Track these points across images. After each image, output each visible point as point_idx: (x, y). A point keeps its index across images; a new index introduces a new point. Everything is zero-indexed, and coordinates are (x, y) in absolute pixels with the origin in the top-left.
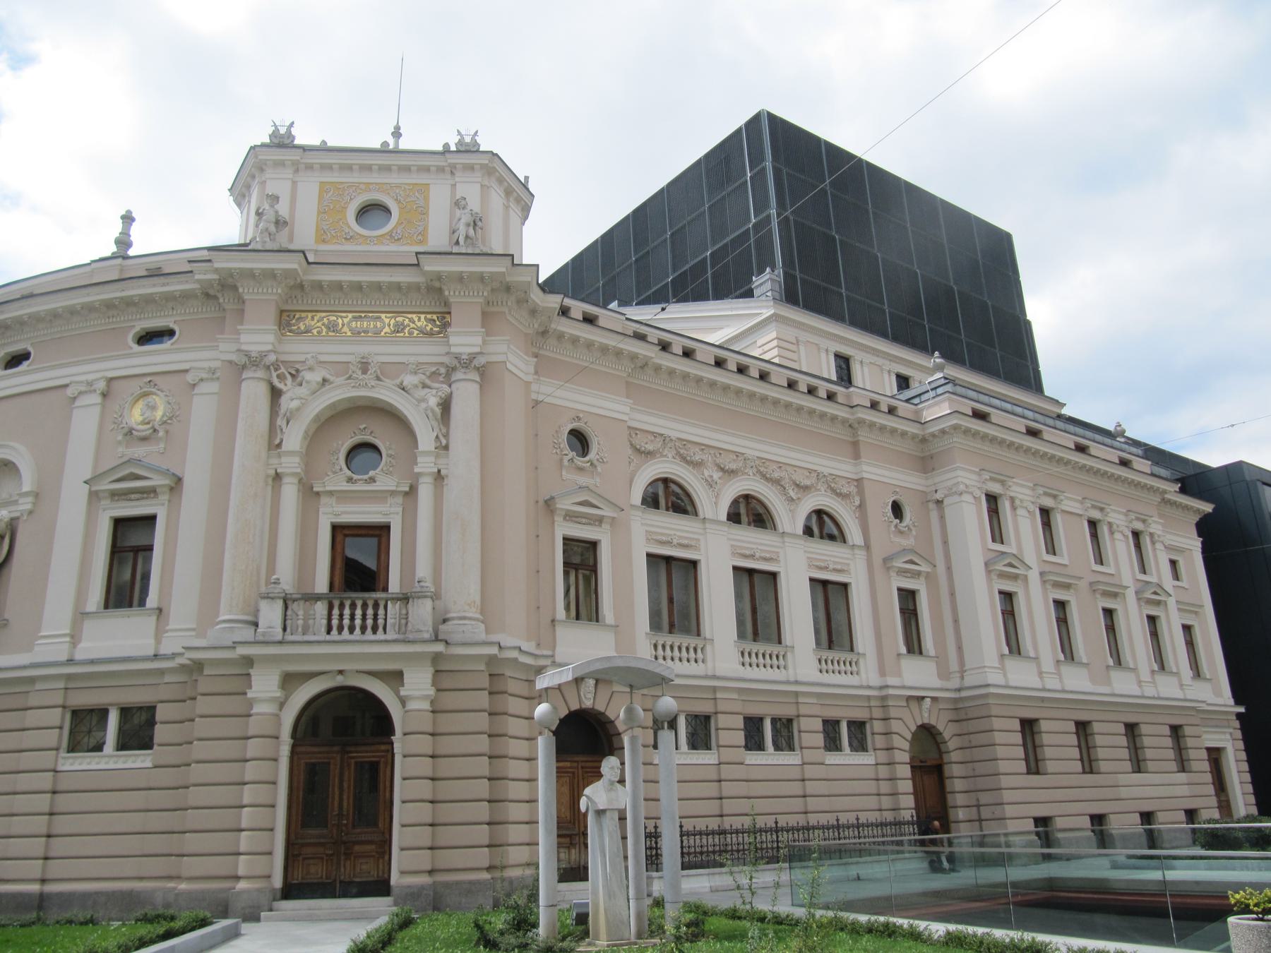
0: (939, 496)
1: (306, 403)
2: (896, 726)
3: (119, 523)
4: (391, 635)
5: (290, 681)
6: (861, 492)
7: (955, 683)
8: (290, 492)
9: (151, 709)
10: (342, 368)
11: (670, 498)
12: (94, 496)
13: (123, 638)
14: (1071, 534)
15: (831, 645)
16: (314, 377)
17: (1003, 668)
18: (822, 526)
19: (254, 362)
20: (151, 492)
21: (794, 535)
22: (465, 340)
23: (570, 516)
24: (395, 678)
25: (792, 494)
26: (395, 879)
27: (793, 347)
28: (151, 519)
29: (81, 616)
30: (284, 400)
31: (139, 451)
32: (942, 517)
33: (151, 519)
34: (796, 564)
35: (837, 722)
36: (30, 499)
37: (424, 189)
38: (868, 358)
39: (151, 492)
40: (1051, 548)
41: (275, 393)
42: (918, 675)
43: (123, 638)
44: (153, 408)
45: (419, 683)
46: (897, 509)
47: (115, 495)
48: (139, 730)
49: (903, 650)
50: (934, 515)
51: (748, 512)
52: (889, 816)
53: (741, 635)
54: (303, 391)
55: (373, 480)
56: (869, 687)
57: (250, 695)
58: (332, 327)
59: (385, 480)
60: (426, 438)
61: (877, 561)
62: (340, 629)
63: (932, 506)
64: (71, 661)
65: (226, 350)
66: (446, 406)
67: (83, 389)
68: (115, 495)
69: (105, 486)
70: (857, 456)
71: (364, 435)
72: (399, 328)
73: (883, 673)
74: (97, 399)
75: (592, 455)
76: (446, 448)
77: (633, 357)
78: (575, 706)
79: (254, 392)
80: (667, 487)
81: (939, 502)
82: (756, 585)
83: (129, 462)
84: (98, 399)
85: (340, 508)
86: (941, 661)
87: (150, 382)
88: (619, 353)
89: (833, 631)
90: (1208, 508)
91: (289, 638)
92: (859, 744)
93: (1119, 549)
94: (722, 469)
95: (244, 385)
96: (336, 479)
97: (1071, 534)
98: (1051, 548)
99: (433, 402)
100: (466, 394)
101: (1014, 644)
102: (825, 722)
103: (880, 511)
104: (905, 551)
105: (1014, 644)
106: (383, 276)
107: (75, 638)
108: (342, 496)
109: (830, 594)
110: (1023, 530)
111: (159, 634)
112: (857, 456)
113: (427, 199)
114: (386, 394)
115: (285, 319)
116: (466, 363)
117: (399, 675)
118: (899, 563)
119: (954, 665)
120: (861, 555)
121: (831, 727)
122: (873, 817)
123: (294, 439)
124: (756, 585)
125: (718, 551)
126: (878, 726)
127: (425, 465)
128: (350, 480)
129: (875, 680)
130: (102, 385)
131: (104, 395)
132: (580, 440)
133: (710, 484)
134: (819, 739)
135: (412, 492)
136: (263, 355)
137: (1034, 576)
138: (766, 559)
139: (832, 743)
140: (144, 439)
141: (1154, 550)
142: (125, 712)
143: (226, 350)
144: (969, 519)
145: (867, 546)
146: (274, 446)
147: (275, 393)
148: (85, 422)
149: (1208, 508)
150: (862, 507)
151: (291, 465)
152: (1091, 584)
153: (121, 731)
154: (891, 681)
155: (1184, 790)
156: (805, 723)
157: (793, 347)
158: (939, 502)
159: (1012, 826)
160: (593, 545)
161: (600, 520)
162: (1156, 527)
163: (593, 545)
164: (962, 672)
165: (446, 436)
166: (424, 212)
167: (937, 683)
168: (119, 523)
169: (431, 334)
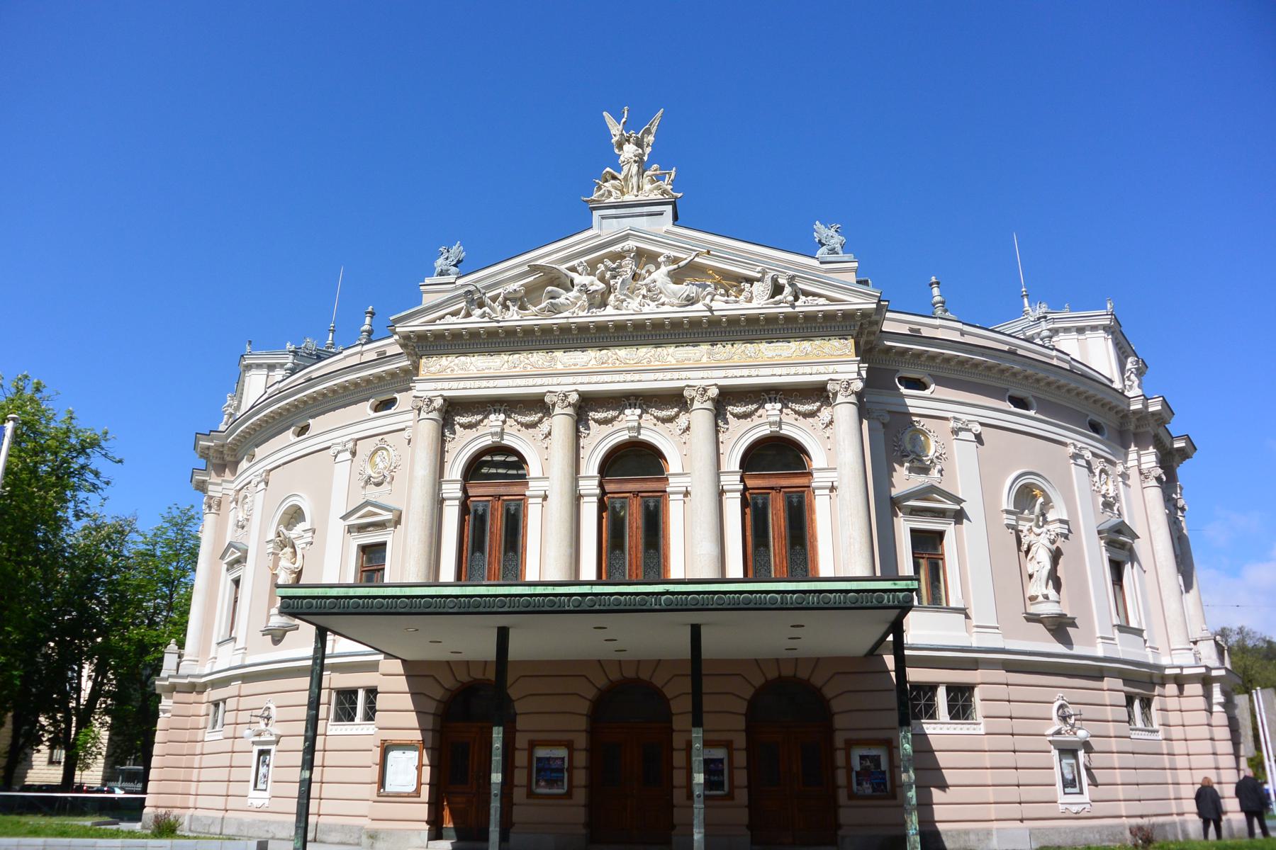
3: (364, 549)
12: (350, 529)
20: (381, 525)
28: (384, 544)
31: (373, 493)
33: (384, 544)
36: (310, 534)
47: (362, 528)
67: (340, 448)
68: (362, 528)
69: (353, 520)
74: (348, 455)
83: (367, 503)
84: (350, 456)
130: (350, 445)
131: (354, 454)
140: (378, 484)
148: (342, 471)
168: (364, 549)
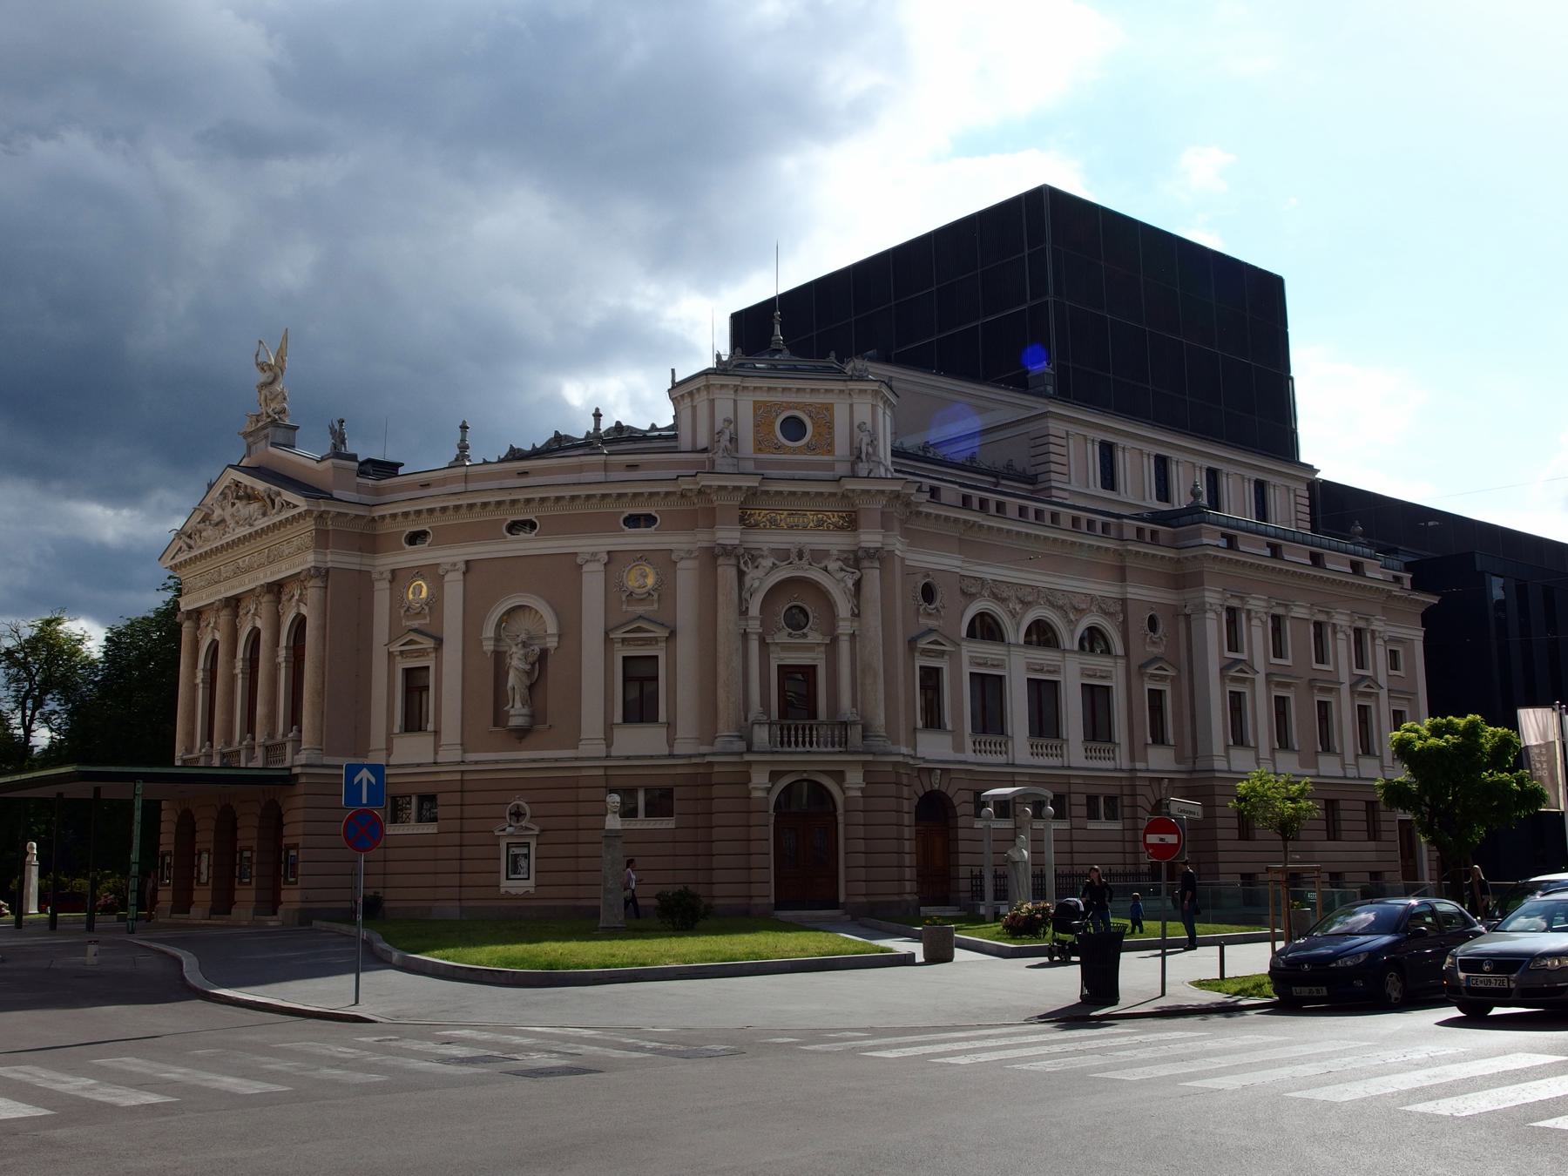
0: (1187, 611)
1: (762, 579)
2: (1140, 800)
4: (837, 749)
5: (775, 776)
6: (1124, 611)
7: (1189, 766)
8: (754, 645)
9: (671, 791)
10: (783, 555)
11: (986, 628)
13: (640, 742)
14: (1298, 639)
15: (1094, 739)
16: (767, 563)
17: (1227, 756)
18: (1093, 640)
19: (728, 551)
21: (1072, 651)
22: (870, 538)
23: (925, 652)
24: (839, 776)
25: (1072, 617)
26: (842, 899)
27: (1063, 442)
28: (656, 657)
29: (609, 727)
30: (747, 579)
32: (1189, 628)
34: (1072, 673)
35: (1097, 797)
37: (829, 408)
38: (1129, 443)
39: (655, 640)
40: (1279, 652)
41: (741, 574)
42: (1160, 760)
43: (640, 742)
44: (646, 576)
45: (855, 779)
46: (1153, 624)
48: (660, 803)
49: (1150, 741)
50: (1182, 625)
51: (1041, 635)
52: (1129, 868)
53: (1032, 733)
54: (760, 573)
55: (805, 635)
56: (1121, 770)
57: (751, 786)
58: (773, 522)
59: (814, 637)
60: (844, 608)
61: (1134, 668)
62: (804, 743)
63: (1181, 618)
64: (608, 757)
65: (702, 539)
66: (858, 584)
70: (1123, 580)
71: (797, 604)
72: (820, 524)
73: (1132, 759)
75: (937, 604)
76: (858, 615)
77: (966, 522)
78: (928, 789)
79: (727, 573)
80: (982, 621)
81: (1187, 616)
82: (1044, 694)
85: (783, 655)
86: (1179, 748)
87: (643, 556)
88: (956, 520)
89: (1098, 728)
90: (1434, 600)
91: (779, 749)
92: (1112, 816)
93: (1341, 648)
94: (1022, 602)
95: (720, 570)
96: (782, 637)
97: (1298, 639)
98: (1279, 652)
99: (850, 584)
100: (873, 577)
101: (1238, 737)
102: (1089, 798)
103: (1139, 624)
104: (1156, 659)
105: (1238, 737)
106: (813, 488)
107: (608, 740)
108: (785, 647)
109: (1097, 698)
110: (1257, 637)
111: (671, 741)
112: (1123, 580)
113: (832, 415)
114: (815, 574)
115: (745, 521)
116: (874, 554)
117: (842, 772)
118: (1151, 670)
119: (1188, 752)
120: (1121, 663)
121: (1092, 801)
122: (1120, 869)
123: (754, 609)
124: (1044, 694)
125: (1017, 666)
126: (1126, 801)
127: (844, 628)
128: (790, 635)
129: (1126, 765)
132: (928, 593)
133: (1013, 614)
134: (1083, 811)
135: (832, 646)
136: (735, 547)
137: (1260, 679)
138: (1050, 672)
139: (1093, 815)
141: (1374, 646)
142: (647, 791)
143: (702, 539)
144: (1213, 629)
145: (1127, 655)
146: (744, 613)
147: (741, 574)
149: (1434, 600)
150: (1125, 622)
151: (754, 626)
152: (1311, 681)
153: (647, 804)
154: (1139, 765)
155: (1372, 856)
156: (1075, 799)
157: (1063, 442)
158: (1187, 616)
159: (1223, 879)
160: (938, 671)
161: (943, 653)
162: (1377, 625)
163: (938, 671)
164: (1195, 758)
165: (858, 606)
166: (830, 426)
167: (1175, 767)
169: (841, 528)
